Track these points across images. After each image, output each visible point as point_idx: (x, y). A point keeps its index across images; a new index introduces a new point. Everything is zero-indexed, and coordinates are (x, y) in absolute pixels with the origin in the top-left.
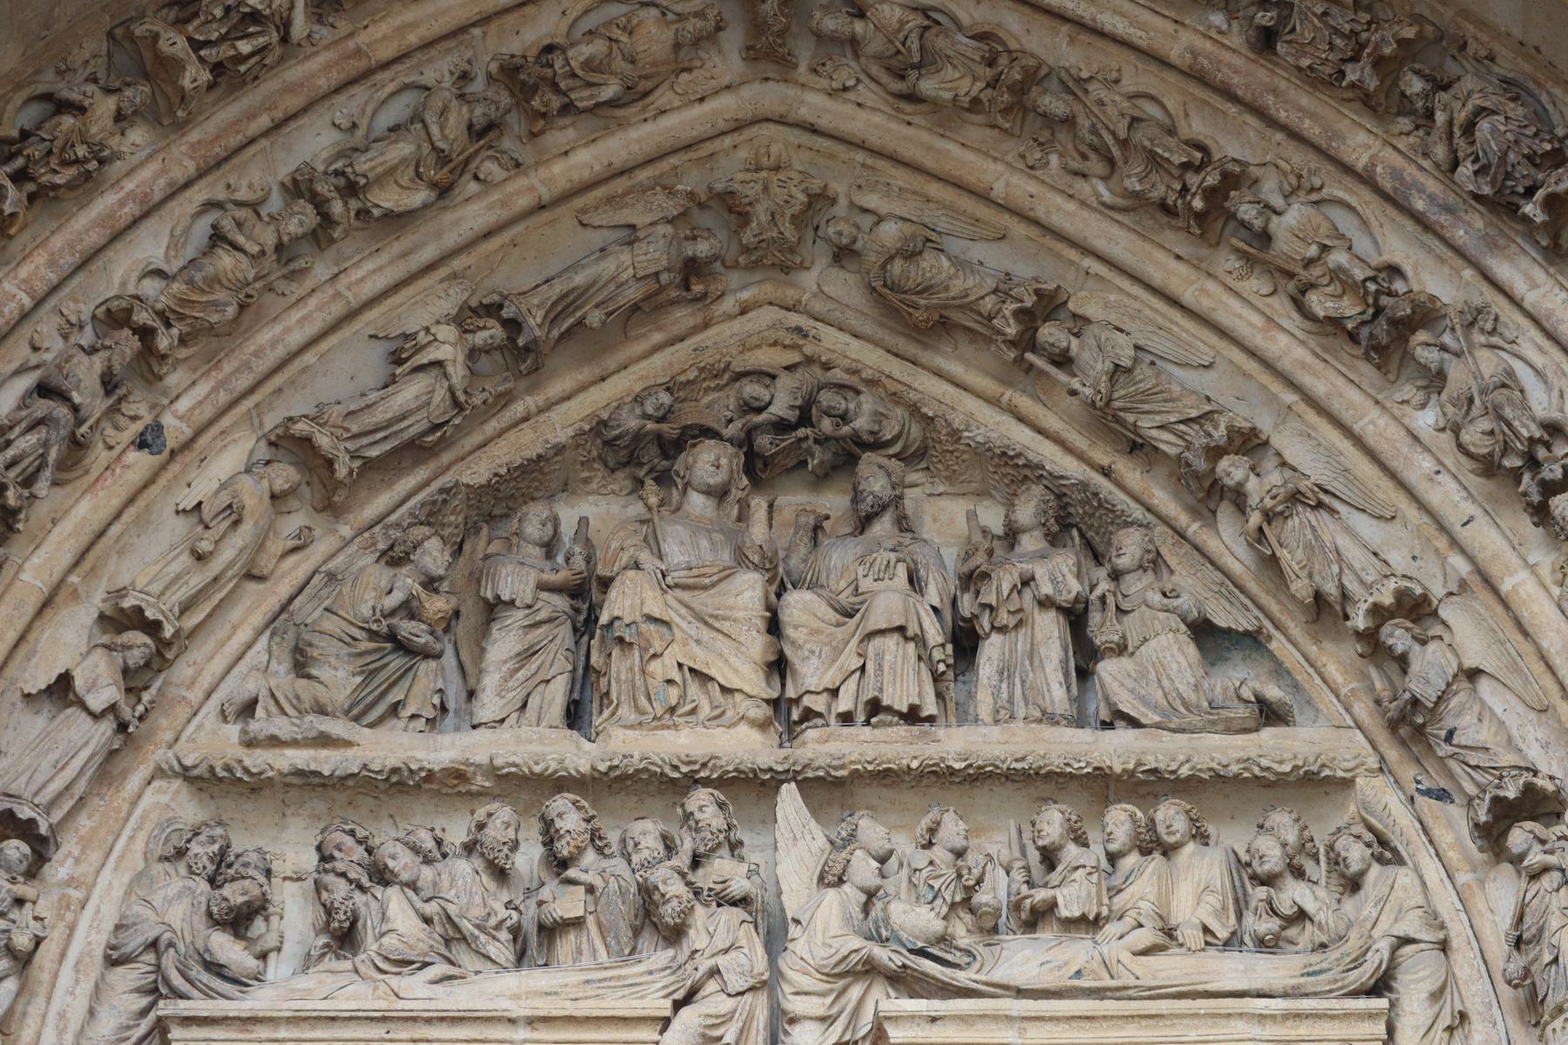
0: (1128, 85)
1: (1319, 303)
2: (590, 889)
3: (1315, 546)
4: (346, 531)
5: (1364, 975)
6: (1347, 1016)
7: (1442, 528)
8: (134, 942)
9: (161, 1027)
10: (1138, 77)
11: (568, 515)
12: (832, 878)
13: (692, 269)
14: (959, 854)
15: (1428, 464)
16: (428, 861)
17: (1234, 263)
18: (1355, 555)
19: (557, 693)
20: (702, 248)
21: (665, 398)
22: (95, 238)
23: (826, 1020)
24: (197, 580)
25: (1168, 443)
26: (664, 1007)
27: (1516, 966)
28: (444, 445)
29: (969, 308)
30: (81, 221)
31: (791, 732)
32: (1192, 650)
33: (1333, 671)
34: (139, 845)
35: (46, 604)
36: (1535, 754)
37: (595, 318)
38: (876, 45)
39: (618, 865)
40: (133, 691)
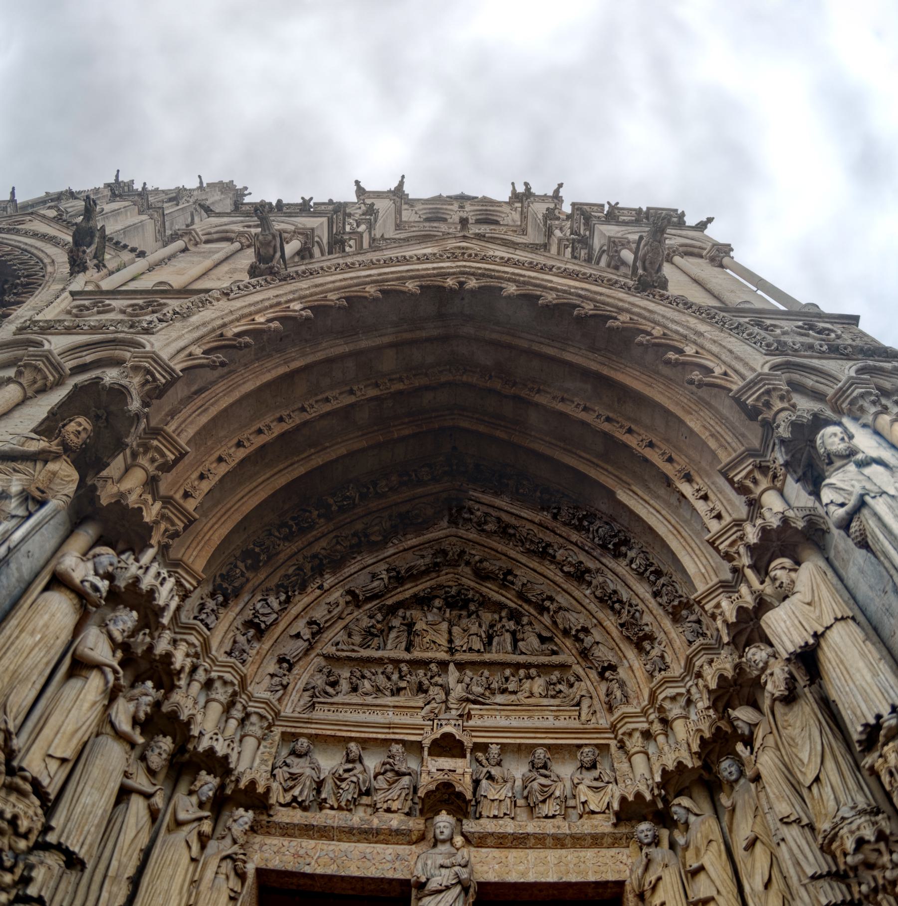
0: (527, 527)
1: (566, 569)
6: (570, 711)
7: (591, 614)
8: (309, 687)
9: (314, 704)
10: (529, 526)
11: (408, 614)
13: (436, 564)
15: (588, 601)
16: (374, 675)
17: (548, 562)
18: (573, 620)
19: (404, 644)
20: (438, 560)
23: (457, 709)
24: (328, 617)
25: (534, 599)
26: (423, 705)
27: (607, 699)
28: (383, 595)
29: (493, 573)
31: (452, 654)
33: (568, 644)
35: (296, 617)
36: (610, 658)
37: (415, 572)
38: (475, 520)
39: (414, 677)
40: (313, 638)
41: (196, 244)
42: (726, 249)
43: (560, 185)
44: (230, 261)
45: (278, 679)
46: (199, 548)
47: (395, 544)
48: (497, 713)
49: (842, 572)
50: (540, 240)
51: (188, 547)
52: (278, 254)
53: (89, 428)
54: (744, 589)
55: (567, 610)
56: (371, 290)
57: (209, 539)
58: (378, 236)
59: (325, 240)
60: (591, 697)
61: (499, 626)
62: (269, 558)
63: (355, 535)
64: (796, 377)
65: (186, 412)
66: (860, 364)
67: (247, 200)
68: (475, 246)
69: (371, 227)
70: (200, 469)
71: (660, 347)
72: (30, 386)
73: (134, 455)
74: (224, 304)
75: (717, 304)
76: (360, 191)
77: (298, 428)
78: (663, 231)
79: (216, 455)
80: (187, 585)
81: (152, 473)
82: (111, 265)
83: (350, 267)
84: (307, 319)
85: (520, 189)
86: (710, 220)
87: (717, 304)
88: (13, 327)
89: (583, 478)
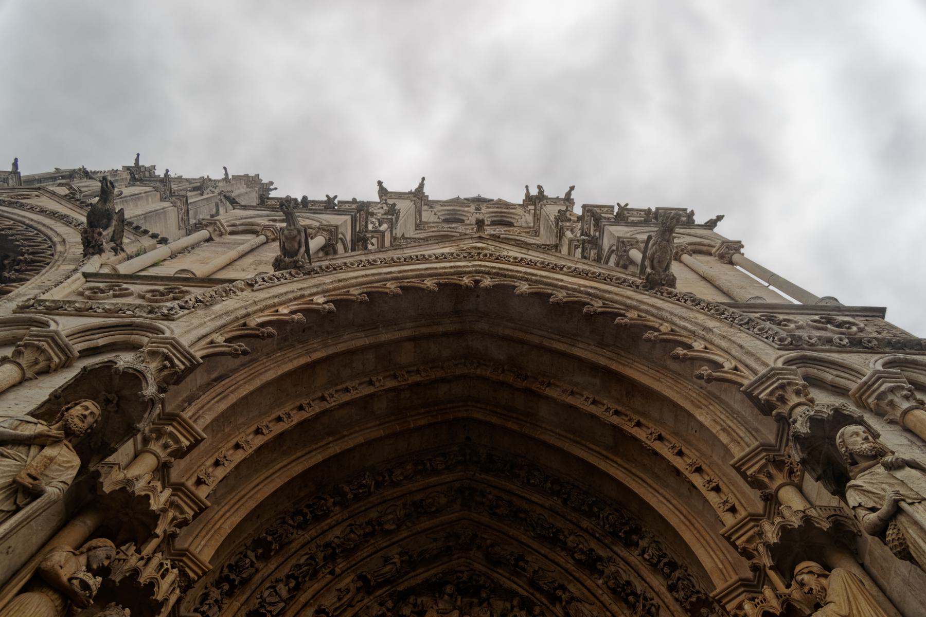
1: (577, 556)
4: (372, 598)
7: (605, 606)
11: (419, 600)
15: (601, 592)
17: (559, 549)
20: (451, 544)
22: (326, 528)
24: (338, 605)
25: (545, 587)
30: (323, 524)
41: (221, 235)
42: (737, 246)
43: (572, 188)
44: (255, 253)
46: (208, 537)
49: (882, 581)
50: (552, 241)
51: (197, 536)
52: (303, 249)
53: (97, 412)
54: (768, 592)
55: (579, 601)
56: (391, 286)
57: (220, 528)
58: (399, 235)
59: (349, 238)
62: (282, 547)
63: (368, 523)
64: (814, 371)
65: (204, 398)
66: (888, 357)
67: (273, 194)
68: (490, 247)
69: (392, 226)
70: (216, 456)
71: (669, 343)
72: (30, 367)
73: (146, 441)
74: (247, 294)
75: (727, 300)
76: (383, 191)
77: (317, 417)
78: (671, 231)
79: (234, 442)
80: (192, 575)
81: (163, 460)
82: (130, 249)
83: (372, 264)
84: (330, 312)
85: (534, 192)
86: (720, 218)
87: (727, 300)
88: (13, 305)
89: (592, 469)
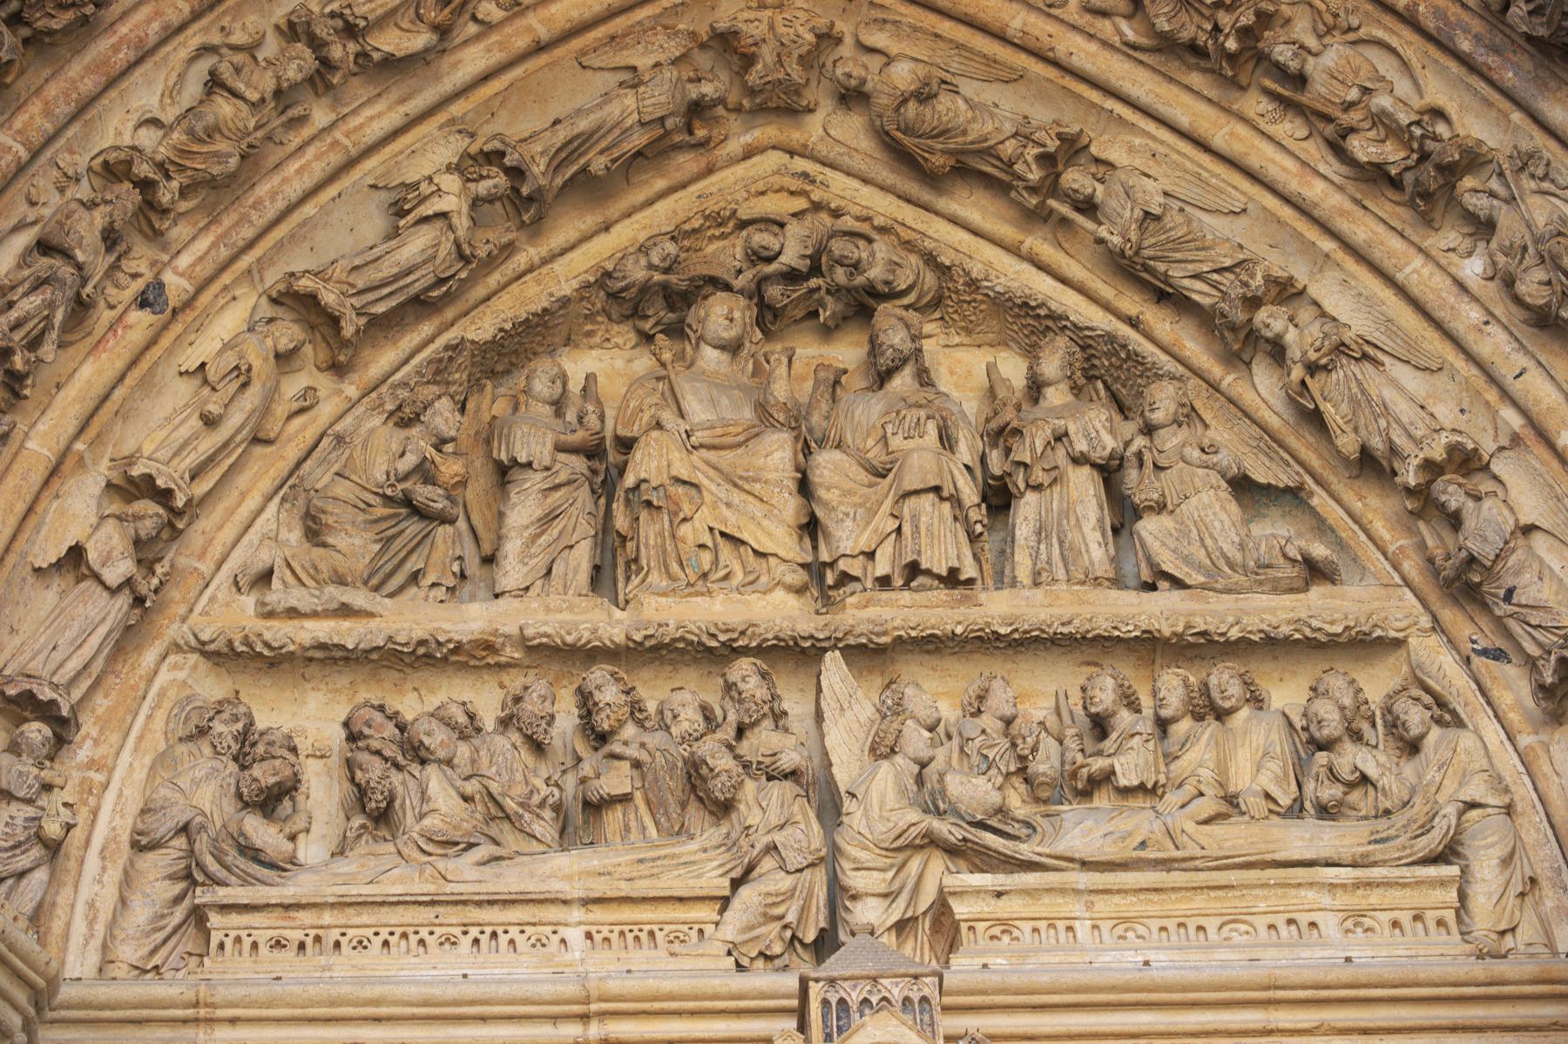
1: (1363, 148)
2: (637, 765)
3: (1361, 400)
4: (352, 391)
5: (1432, 842)
7: (1492, 379)
9: (198, 916)
12: (883, 749)
13: (697, 110)
14: (1008, 722)
15: (1475, 314)
16: (463, 737)
17: (1265, 105)
18: (1403, 409)
19: (582, 557)
20: (708, 89)
21: (671, 248)
22: (89, 85)
23: (889, 896)
25: (1201, 293)
26: (723, 886)
28: (449, 298)
29: (988, 153)
30: (75, 69)
31: (827, 600)
32: (1233, 507)
34: (159, 723)
35: (54, 472)
37: (599, 164)
40: (147, 564)
45: (22, 812)
47: (488, 27)
48: (1075, 907)
55: (1366, 355)
60: (1509, 810)
61: (1039, 438)
